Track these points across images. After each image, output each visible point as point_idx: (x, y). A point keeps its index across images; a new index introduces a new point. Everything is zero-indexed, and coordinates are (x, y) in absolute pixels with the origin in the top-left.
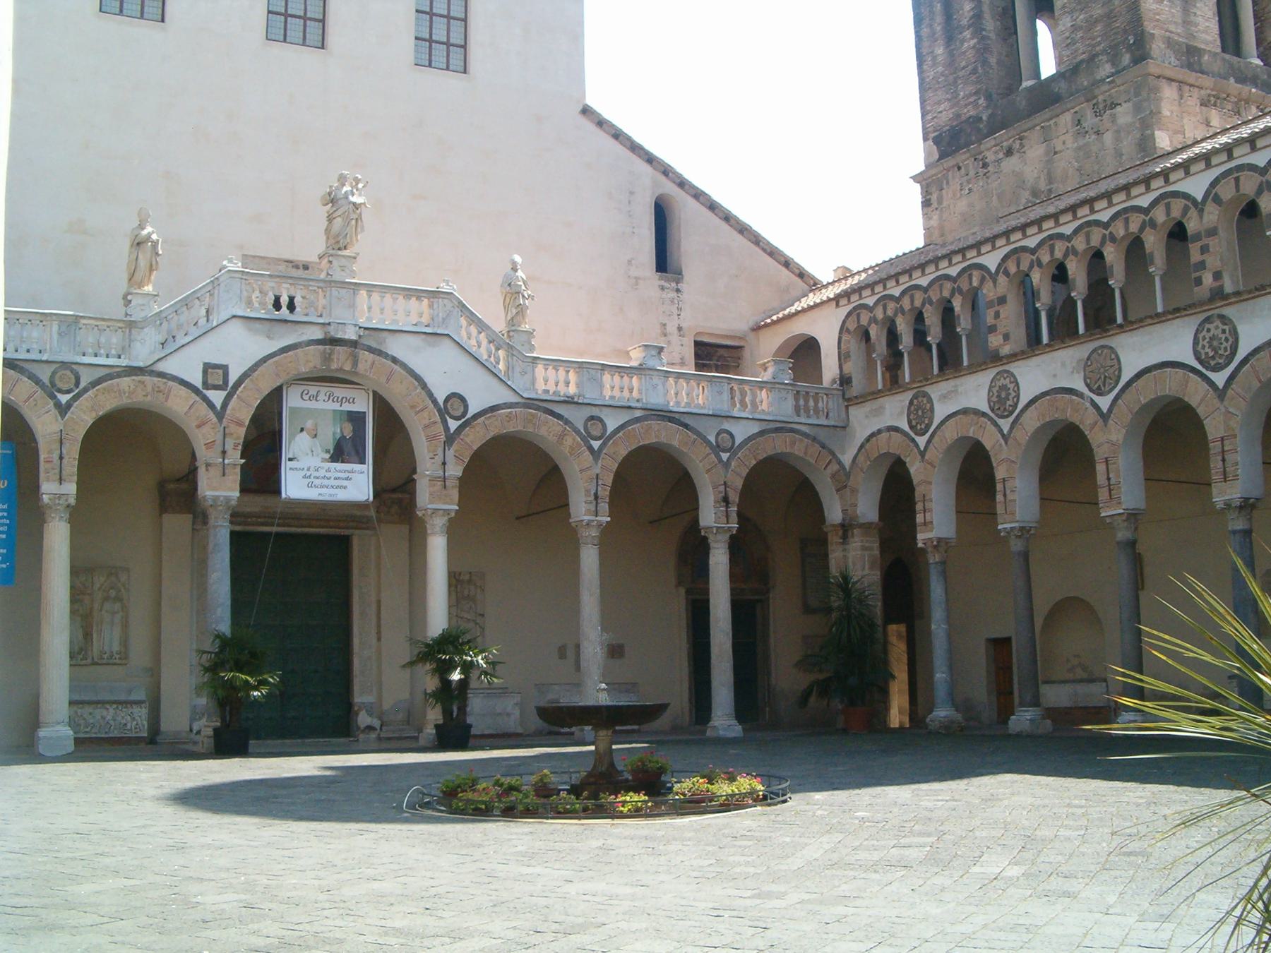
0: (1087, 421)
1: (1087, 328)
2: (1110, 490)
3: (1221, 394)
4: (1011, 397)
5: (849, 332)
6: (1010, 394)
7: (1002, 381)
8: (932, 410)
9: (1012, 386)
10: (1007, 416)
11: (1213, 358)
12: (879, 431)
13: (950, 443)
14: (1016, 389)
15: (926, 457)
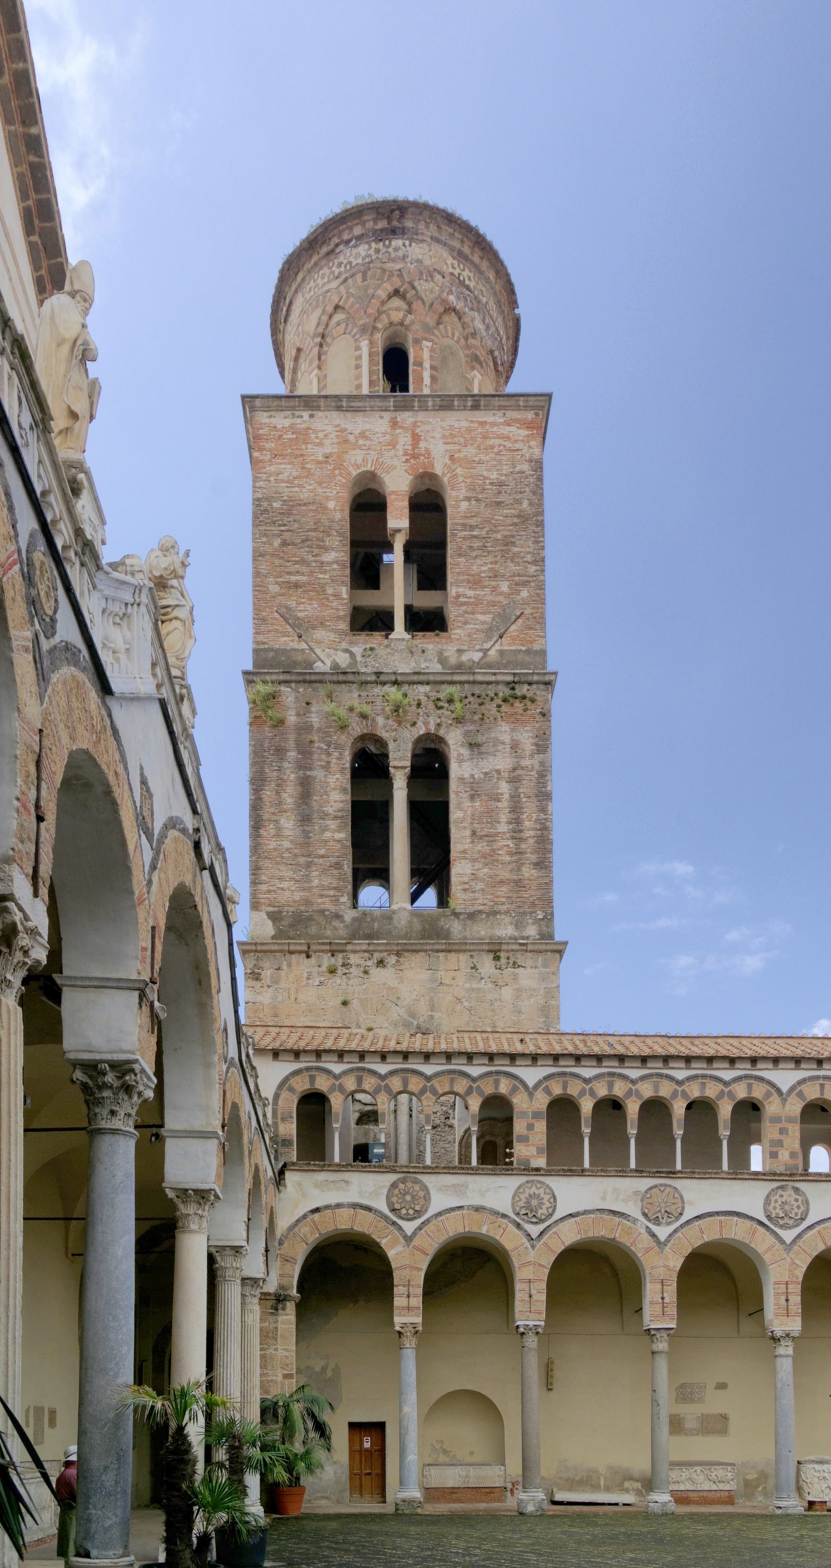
0: (640, 1246)
1: (592, 1163)
2: (663, 1307)
3: (789, 1247)
4: (544, 1207)
5: (291, 1090)
6: (543, 1204)
7: (534, 1190)
8: (427, 1198)
9: (546, 1197)
10: (536, 1223)
11: (782, 1218)
12: (338, 1206)
13: (451, 1235)
14: (552, 1200)
15: (416, 1242)
